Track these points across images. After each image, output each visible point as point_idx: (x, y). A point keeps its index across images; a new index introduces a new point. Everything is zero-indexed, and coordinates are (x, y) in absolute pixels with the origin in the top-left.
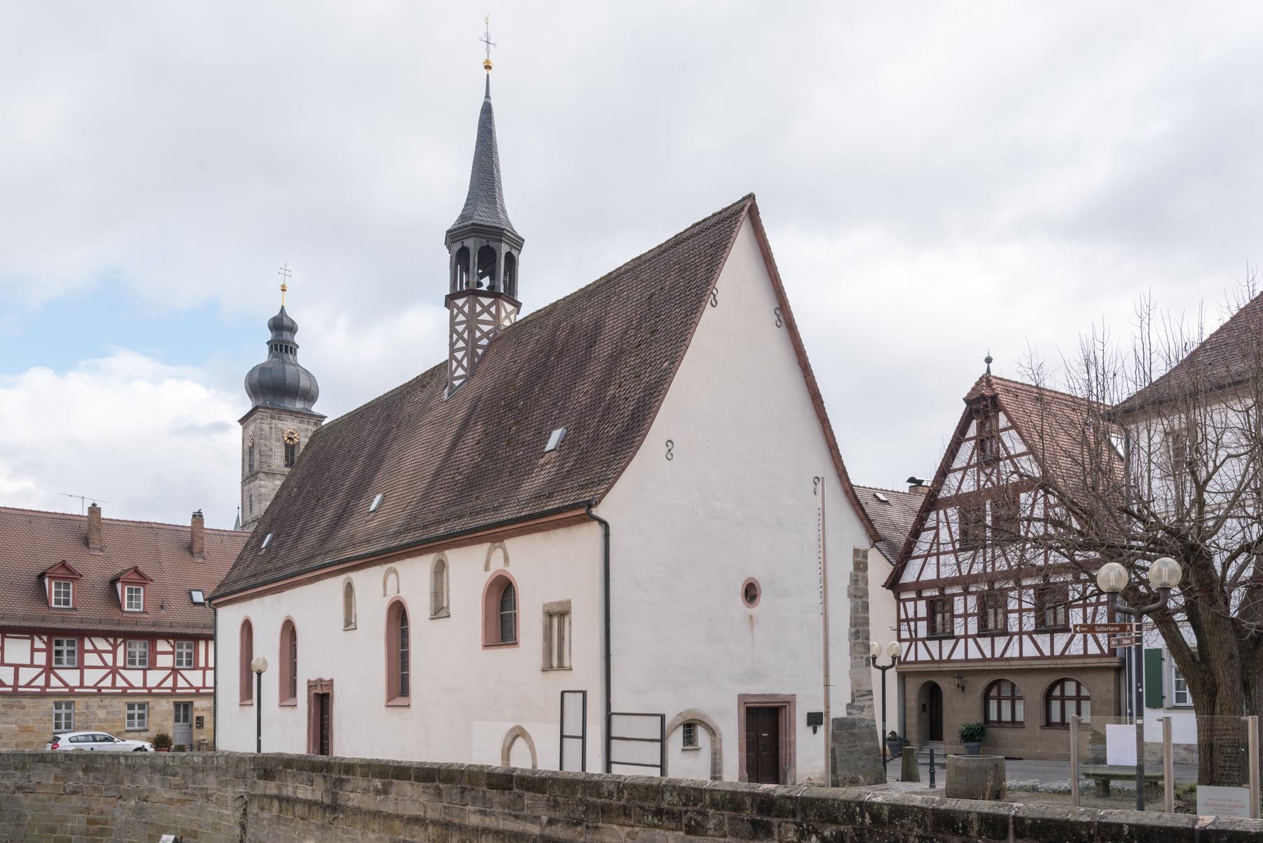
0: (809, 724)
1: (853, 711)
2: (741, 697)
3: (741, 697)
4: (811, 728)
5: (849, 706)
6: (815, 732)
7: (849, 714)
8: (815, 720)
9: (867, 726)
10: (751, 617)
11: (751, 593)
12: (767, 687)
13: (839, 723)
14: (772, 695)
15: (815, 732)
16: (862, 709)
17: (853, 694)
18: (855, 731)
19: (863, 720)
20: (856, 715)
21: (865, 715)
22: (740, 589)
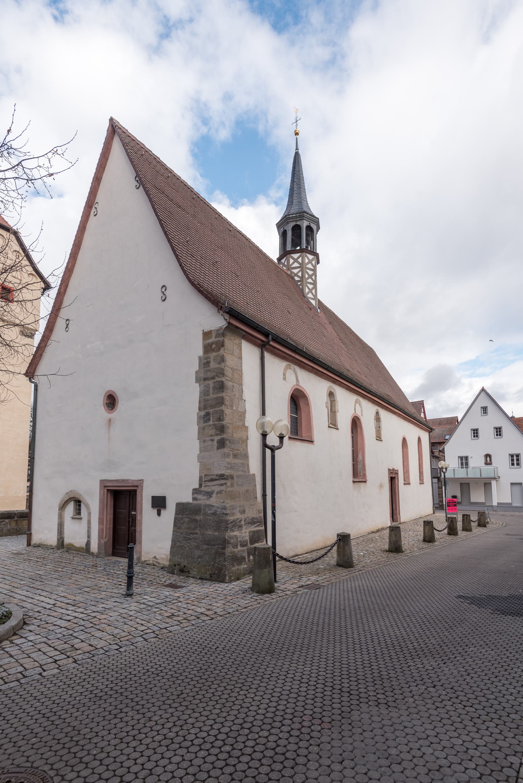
0: (154, 506)
1: (199, 497)
2: (102, 482)
3: (102, 482)
4: (155, 511)
5: (195, 491)
6: (159, 514)
7: (194, 499)
8: (159, 503)
9: (214, 514)
10: (110, 420)
11: (111, 401)
12: (123, 474)
13: (182, 509)
14: (123, 481)
15: (159, 514)
16: (209, 494)
17: (201, 478)
18: (198, 518)
19: (210, 506)
20: (203, 500)
21: (214, 501)
22: (101, 400)
